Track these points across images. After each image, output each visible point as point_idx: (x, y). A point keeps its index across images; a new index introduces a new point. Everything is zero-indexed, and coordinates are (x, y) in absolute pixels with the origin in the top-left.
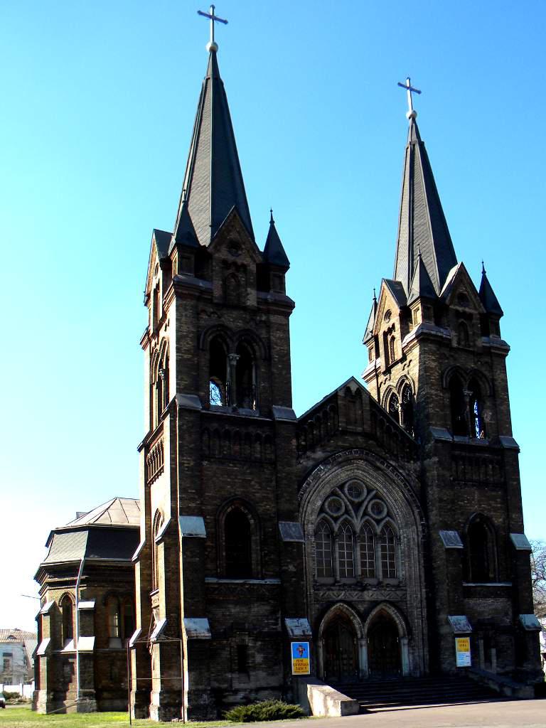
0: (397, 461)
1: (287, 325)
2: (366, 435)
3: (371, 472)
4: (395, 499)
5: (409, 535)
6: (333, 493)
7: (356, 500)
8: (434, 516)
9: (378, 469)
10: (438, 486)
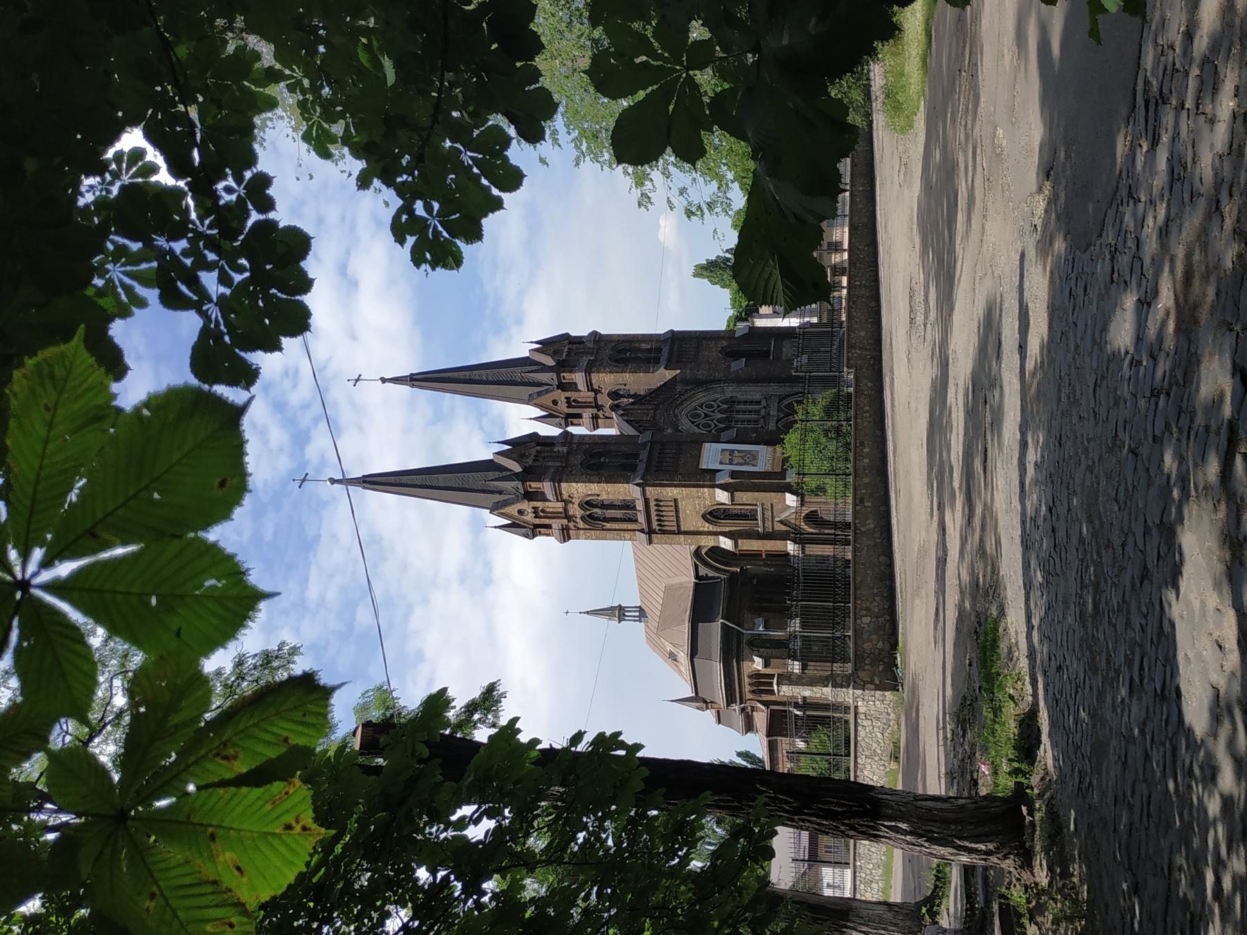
0: (675, 395)
1: (580, 435)
2: (655, 410)
3: (683, 406)
4: (702, 397)
5: (730, 391)
6: (698, 426)
7: (703, 415)
8: (718, 375)
9: (681, 403)
10: (698, 371)
